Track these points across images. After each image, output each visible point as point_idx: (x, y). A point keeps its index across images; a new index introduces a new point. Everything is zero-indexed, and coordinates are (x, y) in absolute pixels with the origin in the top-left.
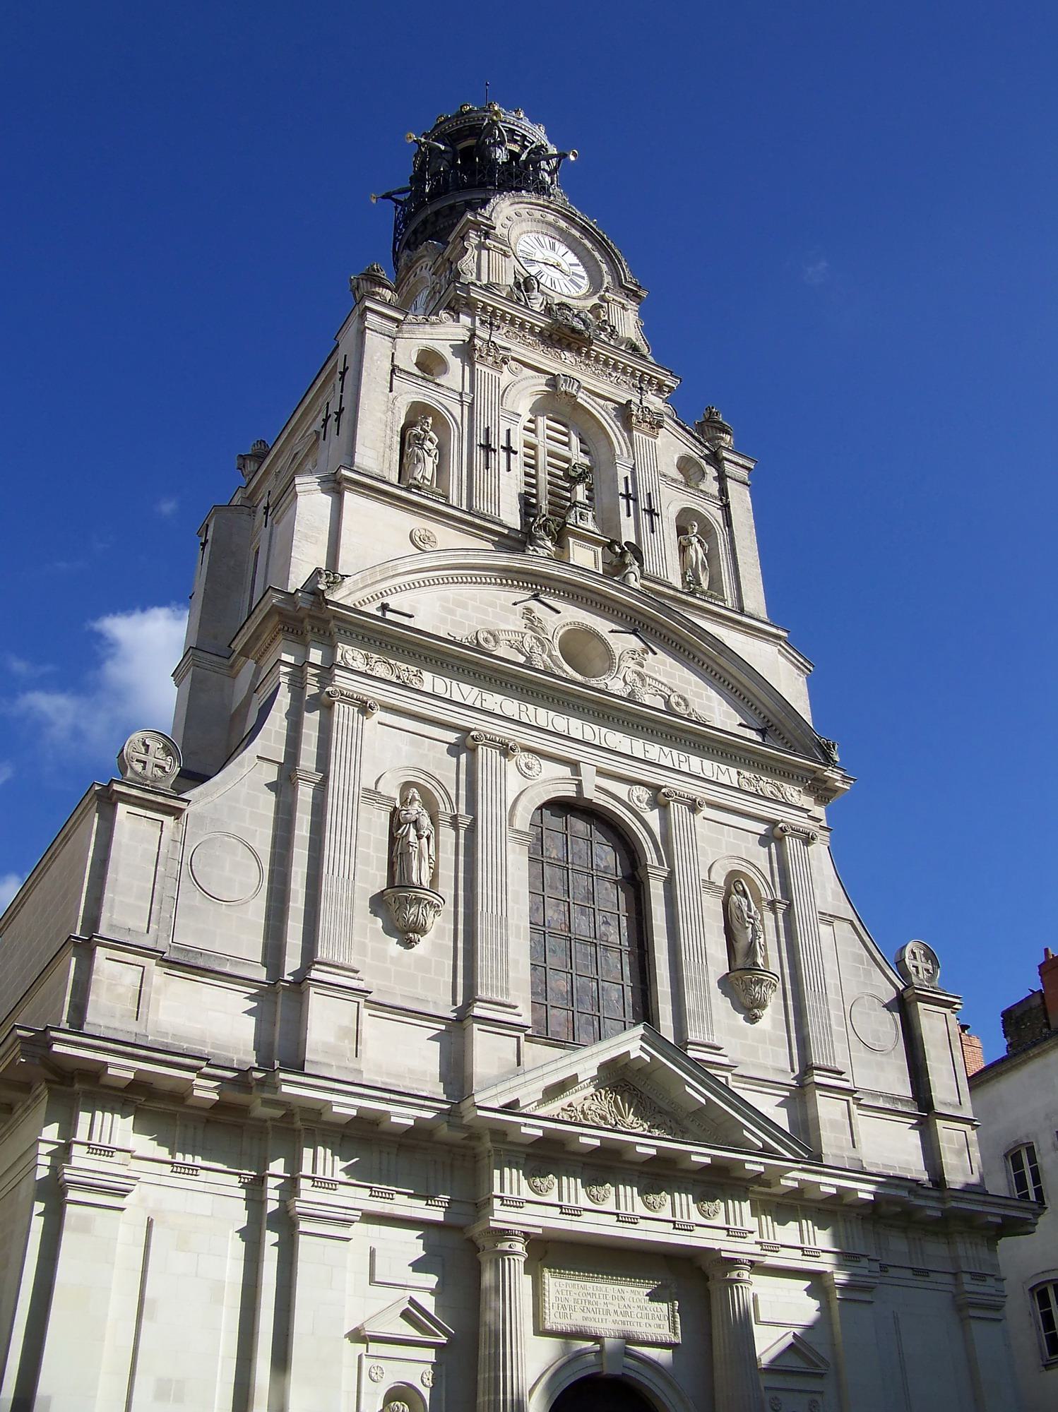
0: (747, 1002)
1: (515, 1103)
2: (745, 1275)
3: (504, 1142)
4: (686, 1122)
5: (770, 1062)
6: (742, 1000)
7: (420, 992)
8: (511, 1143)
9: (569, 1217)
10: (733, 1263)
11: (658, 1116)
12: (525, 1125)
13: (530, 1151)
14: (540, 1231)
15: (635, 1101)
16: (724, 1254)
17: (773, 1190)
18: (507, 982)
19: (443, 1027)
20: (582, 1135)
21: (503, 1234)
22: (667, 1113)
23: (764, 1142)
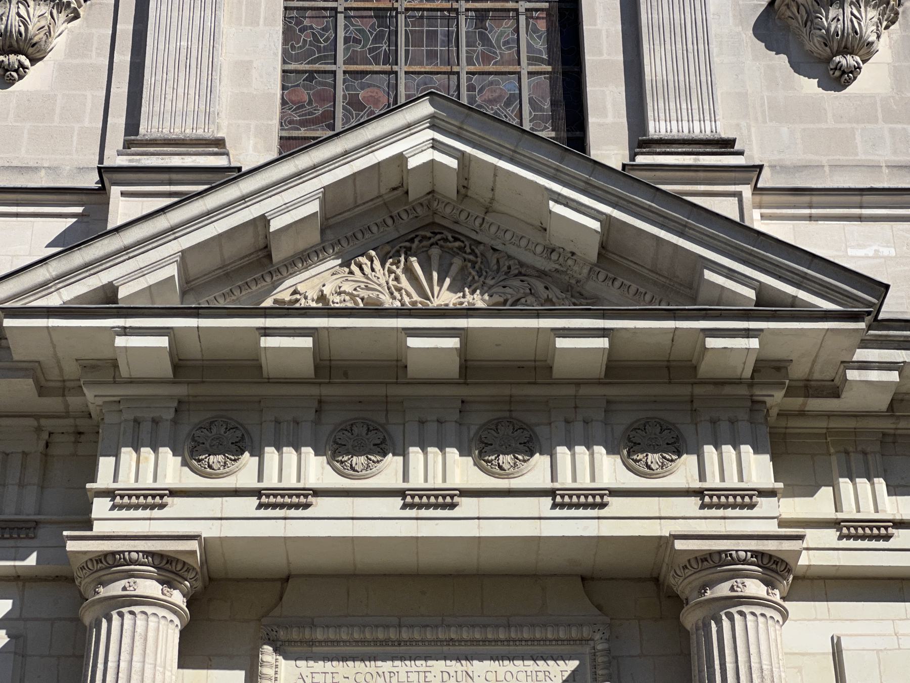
0: (815, 45)
1: (109, 292)
2: (754, 588)
3: (116, 381)
4: (591, 287)
5: (885, 155)
6: (809, 46)
7: (24, 155)
8: (131, 381)
9: (278, 513)
10: (715, 564)
11: (516, 283)
12: (125, 331)
13: (181, 390)
14: (194, 545)
15: (457, 262)
16: (679, 545)
17: (848, 401)
18: (209, 102)
19: (79, 210)
20: (267, 332)
21: (110, 564)
22: (542, 274)
23: (760, 289)
